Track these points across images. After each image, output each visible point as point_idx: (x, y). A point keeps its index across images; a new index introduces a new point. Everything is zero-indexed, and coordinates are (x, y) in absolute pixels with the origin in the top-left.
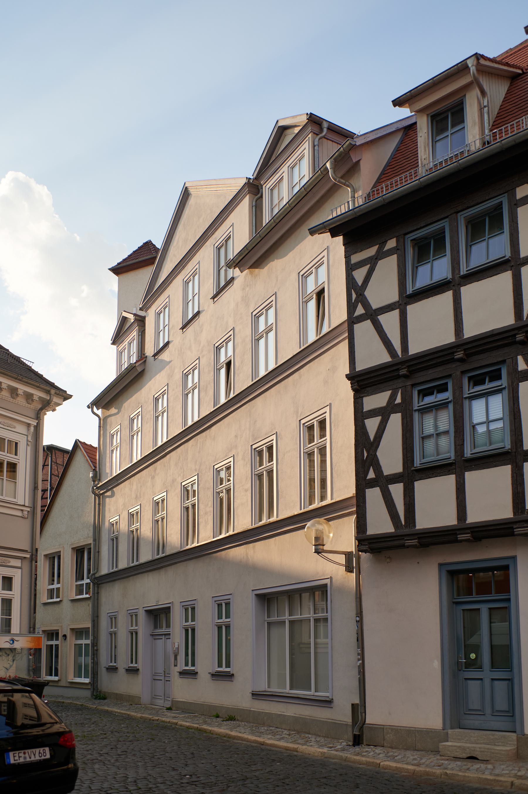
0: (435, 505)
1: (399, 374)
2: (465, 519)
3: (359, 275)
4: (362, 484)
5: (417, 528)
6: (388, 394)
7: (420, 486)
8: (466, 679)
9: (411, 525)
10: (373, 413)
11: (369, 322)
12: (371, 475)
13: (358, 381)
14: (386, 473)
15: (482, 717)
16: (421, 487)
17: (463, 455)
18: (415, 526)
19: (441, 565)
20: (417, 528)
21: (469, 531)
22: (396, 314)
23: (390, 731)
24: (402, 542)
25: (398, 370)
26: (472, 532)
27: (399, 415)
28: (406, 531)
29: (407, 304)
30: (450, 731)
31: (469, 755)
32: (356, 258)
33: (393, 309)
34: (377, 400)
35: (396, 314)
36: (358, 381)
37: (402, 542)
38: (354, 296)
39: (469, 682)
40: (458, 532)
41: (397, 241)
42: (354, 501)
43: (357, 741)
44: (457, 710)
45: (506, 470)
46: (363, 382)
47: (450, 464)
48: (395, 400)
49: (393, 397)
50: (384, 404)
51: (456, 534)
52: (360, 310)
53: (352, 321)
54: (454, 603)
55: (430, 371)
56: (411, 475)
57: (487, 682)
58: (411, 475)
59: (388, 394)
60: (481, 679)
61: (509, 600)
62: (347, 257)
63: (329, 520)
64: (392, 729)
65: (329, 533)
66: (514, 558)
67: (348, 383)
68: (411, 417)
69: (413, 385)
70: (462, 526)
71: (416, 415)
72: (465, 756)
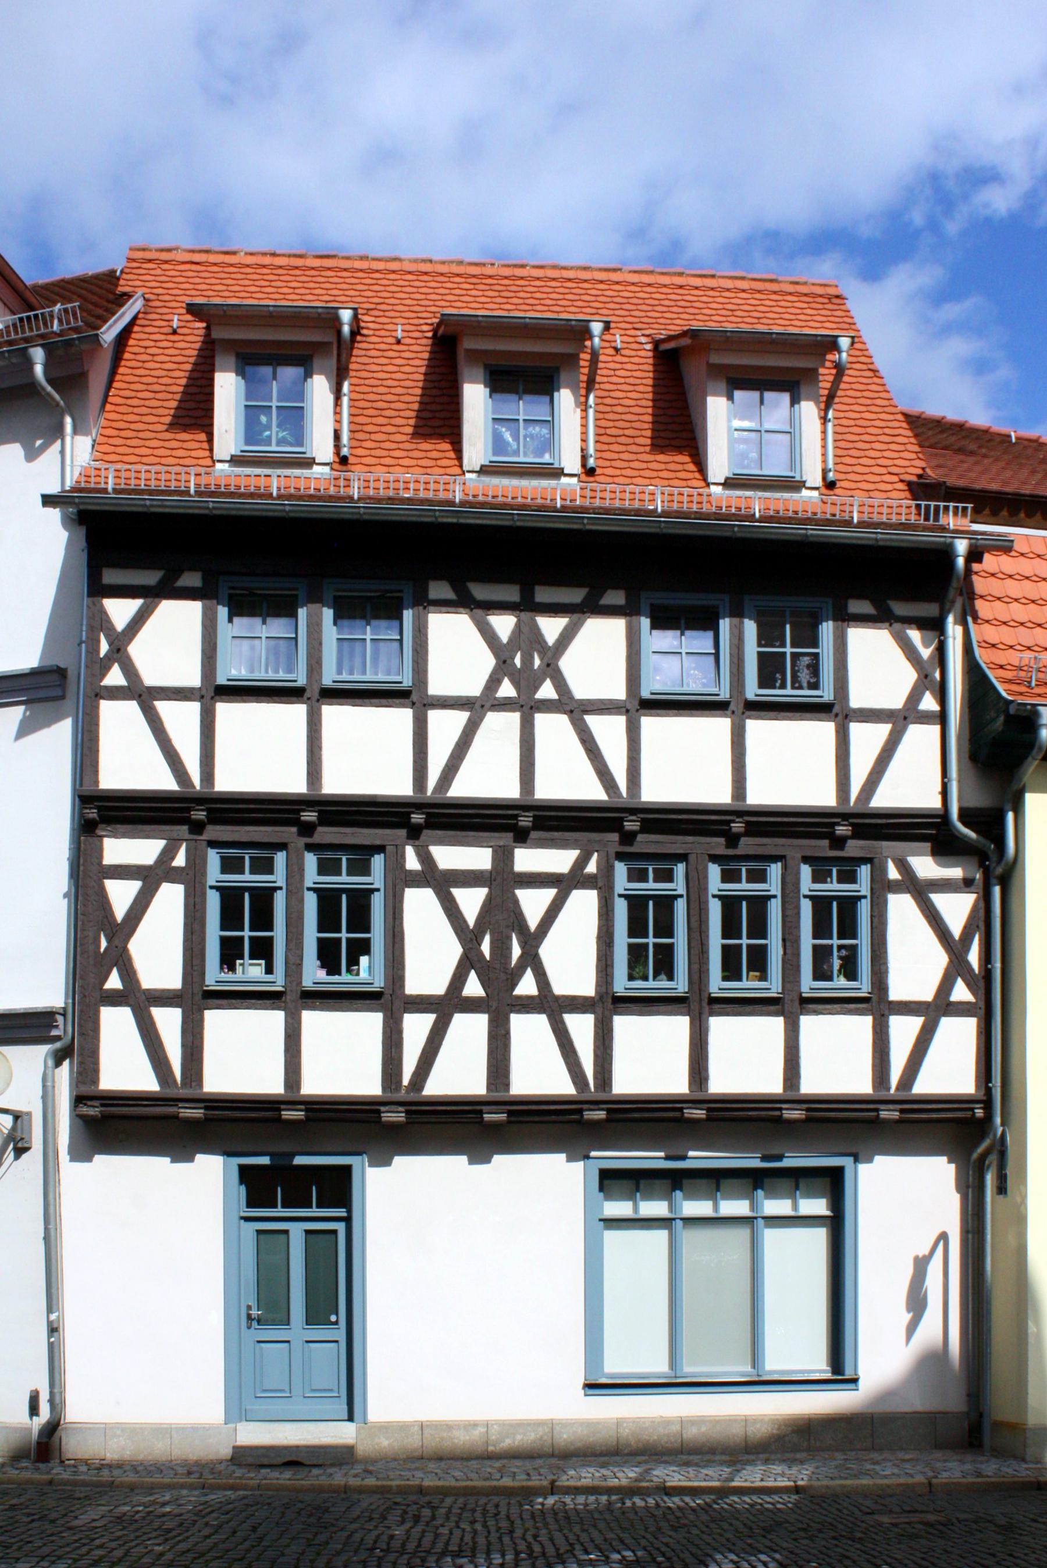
0: (242, 1053)
1: (189, 817)
9: (194, 1084)
21: (303, 1107)
23: (119, 1432)
24: (172, 1110)
31: (286, 1460)
37: (172, 1110)
38: (104, 647)
40: (283, 1107)
46: (102, 812)
48: (173, 859)
49: (168, 854)
51: (280, 1110)
56: (196, 998)
58: (196, 998)
64: (123, 1430)
70: (292, 1097)
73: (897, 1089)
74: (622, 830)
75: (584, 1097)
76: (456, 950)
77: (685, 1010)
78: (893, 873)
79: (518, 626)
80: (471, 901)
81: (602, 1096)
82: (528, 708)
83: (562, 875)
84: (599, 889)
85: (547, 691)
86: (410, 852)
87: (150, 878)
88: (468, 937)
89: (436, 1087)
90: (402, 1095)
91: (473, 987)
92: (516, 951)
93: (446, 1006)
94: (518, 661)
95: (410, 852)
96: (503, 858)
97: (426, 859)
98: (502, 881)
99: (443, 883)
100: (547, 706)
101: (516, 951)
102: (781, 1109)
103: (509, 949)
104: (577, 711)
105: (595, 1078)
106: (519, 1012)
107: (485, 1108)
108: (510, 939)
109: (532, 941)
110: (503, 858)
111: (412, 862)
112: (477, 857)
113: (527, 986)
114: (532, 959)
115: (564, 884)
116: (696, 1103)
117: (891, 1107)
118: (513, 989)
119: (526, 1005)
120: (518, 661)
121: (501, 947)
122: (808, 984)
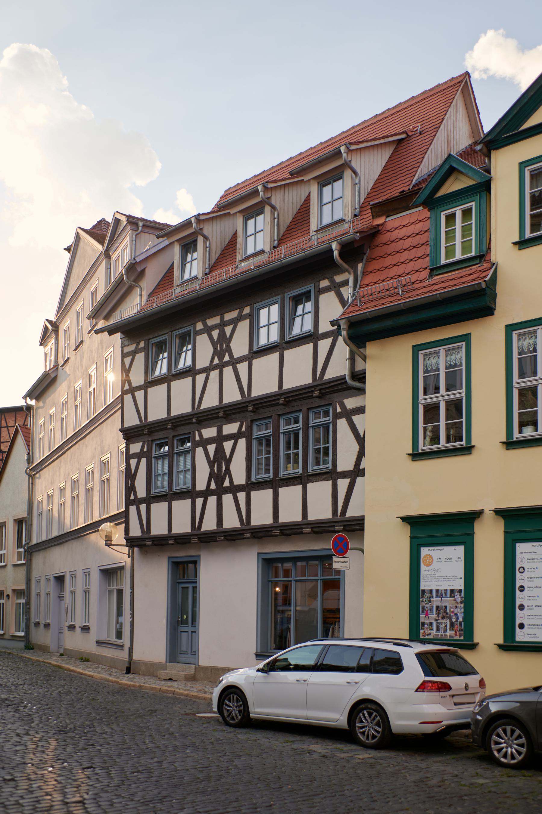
2: (171, 531)
3: (127, 360)
4: (128, 502)
5: (152, 534)
6: (140, 444)
7: (153, 506)
8: (181, 631)
10: (135, 456)
11: (130, 395)
12: (132, 497)
13: (126, 434)
14: (139, 497)
15: (187, 656)
16: (153, 506)
17: (172, 491)
18: (150, 533)
19: (169, 558)
20: (152, 534)
22: (142, 392)
25: (143, 430)
26: (175, 539)
27: (145, 459)
28: (146, 536)
29: (148, 387)
30: (168, 664)
32: (126, 350)
33: (141, 389)
34: (136, 448)
35: (142, 392)
36: (126, 434)
39: (183, 633)
41: (145, 343)
42: (124, 514)
43: (128, 671)
44: (174, 651)
45: (189, 502)
46: (130, 434)
47: (166, 495)
50: (138, 451)
52: (127, 387)
53: (124, 393)
54: (177, 582)
55: (160, 433)
57: (190, 633)
59: (140, 444)
60: (187, 632)
61: (196, 582)
62: (122, 348)
63: (116, 525)
64: (144, 663)
65: (115, 534)
66: (199, 556)
67: (121, 435)
68: (151, 461)
69: (152, 441)
71: (154, 460)
72: (168, 678)
73: (340, 515)
74: (252, 410)
75: (243, 528)
76: (208, 470)
77: (271, 486)
78: (339, 410)
79: (219, 333)
80: (212, 448)
81: (248, 527)
82: (221, 367)
83: (235, 434)
84: (246, 437)
85: (227, 358)
86: (196, 432)
87: (139, 456)
88: (211, 464)
89: (204, 528)
90: (196, 532)
91: (213, 486)
92: (224, 468)
93: (206, 494)
94: (219, 348)
95: (196, 432)
96: (220, 431)
97: (201, 435)
98: (220, 439)
99: (204, 443)
100: (227, 364)
101: (224, 468)
102: (302, 528)
103: (222, 468)
104: (234, 362)
105: (246, 519)
106: (225, 494)
107: (217, 535)
108: (222, 463)
109: (228, 462)
110: (220, 431)
111: (197, 438)
112: (210, 432)
113: (227, 483)
114: (228, 470)
115: (235, 437)
116: (276, 527)
117: (339, 524)
118: (223, 484)
119: (227, 491)
120: (219, 348)
121: (220, 468)
122: (311, 468)
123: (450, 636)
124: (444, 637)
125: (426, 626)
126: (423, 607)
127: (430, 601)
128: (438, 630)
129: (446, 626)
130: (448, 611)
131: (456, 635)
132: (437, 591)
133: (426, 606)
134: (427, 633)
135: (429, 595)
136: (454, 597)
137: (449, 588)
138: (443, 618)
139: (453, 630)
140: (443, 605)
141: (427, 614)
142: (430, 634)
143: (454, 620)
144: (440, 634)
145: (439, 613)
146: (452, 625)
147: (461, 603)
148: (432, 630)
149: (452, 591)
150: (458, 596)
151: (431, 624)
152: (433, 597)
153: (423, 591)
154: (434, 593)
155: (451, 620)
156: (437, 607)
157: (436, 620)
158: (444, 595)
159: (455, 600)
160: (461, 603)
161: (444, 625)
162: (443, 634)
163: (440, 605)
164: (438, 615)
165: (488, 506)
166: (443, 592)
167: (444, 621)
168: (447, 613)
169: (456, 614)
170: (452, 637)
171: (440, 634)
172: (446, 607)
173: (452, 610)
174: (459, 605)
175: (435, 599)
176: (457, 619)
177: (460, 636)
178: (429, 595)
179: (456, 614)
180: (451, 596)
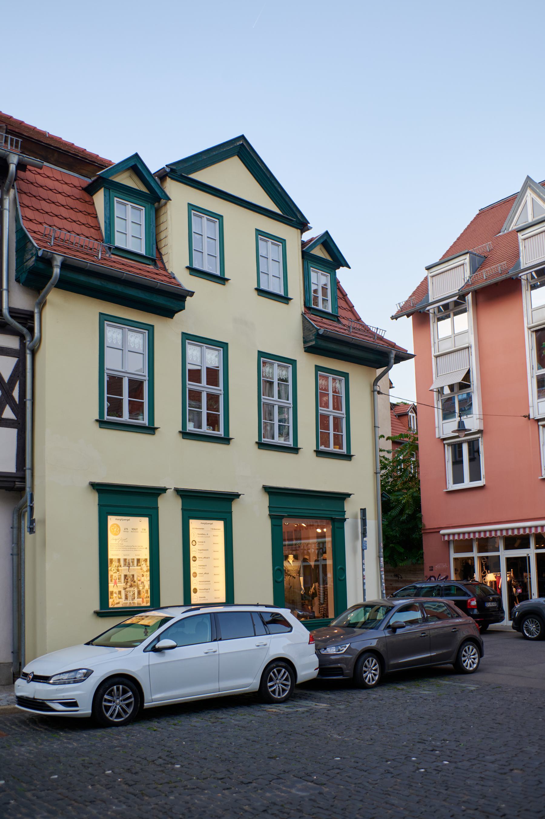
123: (138, 603)
124: (132, 605)
125: (114, 595)
126: (112, 576)
127: (118, 570)
128: (126, 598)
129: (134, 594)
130: (135, 579)
131: (143, 602)
132: (125, 560)
133: (114, 575)
134: (116, 602)
135: (117, 564)
136: (140, 566)
137: (136, 558)
138: (131, 586)
139: (140, 598)
140: (131, 574)
141: (115, 583)
142: (118, 603)
143: (141, 588)
144: (128, 602)
145: (127, 582)
146: (139, 592)
147: (147, 571)
148: (120, 598)
149: (138, 560)
150: (144, 565)
151: (120, 592)
152: (120, 566)
153: (112, 560)
154: (122, 562)
155: (138, 587)
156: (126, 576)
157: (125, 589)
158: (131, 564)
159: (141, 569)
160: (147, 571)
161: (132, 593)
162: (131, 602)
163: (128, 573)
164: (126, 584)
165: (170, 482)
166: (130, 561)
167: (132, 589)
168: (134, 582)
169: (142, 582)
170: (140, 604)
171: (128, 602)
172: (133, 576)
173: (139, 578)
174: (145, 574)
175: (123, 568)
176: (144, 586)
177: (147, 603)
178: (117, 564)
179: (142, 582)
180: (137, 565)
